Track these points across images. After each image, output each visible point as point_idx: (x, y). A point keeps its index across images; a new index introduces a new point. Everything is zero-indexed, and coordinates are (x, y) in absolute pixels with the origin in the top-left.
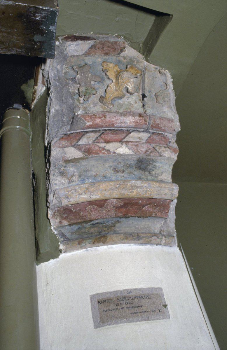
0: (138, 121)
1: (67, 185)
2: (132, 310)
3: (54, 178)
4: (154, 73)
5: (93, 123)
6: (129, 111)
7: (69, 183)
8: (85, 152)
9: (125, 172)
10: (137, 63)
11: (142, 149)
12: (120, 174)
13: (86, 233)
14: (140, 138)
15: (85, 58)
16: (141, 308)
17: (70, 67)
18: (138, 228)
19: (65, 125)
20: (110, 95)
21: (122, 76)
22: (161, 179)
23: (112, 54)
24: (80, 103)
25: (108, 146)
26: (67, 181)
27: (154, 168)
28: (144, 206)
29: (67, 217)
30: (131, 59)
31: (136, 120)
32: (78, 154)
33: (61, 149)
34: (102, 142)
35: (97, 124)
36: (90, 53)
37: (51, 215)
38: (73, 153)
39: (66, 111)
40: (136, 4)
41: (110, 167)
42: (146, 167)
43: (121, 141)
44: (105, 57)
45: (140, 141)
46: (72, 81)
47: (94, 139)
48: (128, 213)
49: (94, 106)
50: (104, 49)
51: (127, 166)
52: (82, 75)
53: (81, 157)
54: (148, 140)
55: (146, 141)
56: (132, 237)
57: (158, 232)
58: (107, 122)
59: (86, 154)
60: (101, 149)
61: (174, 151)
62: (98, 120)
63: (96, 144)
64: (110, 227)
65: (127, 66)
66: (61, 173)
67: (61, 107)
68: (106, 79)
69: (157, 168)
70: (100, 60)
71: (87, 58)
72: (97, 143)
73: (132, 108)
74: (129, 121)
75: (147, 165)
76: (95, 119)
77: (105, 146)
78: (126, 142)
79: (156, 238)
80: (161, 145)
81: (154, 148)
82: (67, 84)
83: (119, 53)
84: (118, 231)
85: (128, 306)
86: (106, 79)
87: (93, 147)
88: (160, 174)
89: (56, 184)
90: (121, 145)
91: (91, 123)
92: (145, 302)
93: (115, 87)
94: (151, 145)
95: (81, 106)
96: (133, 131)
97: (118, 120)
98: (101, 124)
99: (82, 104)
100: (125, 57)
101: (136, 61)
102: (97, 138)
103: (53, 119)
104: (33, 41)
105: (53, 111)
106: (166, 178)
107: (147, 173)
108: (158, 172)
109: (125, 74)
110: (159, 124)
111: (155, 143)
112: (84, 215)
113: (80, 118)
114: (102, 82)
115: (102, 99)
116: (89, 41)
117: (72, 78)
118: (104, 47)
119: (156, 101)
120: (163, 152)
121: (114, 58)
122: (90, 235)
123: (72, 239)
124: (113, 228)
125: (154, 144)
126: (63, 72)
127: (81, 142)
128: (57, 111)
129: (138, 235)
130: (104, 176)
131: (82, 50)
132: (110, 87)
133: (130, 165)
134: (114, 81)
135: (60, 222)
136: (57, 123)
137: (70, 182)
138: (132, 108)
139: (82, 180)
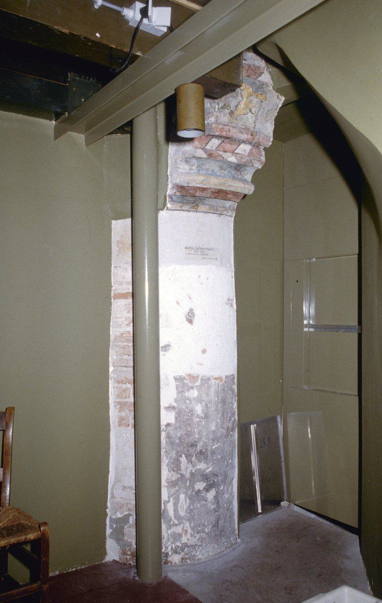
1: (188, 171)
2: (203, 257)
7: (190, 170)
14: (244, 151)
25: (224, 155)
32: (204, 155)
43: (233, 152)
72: (219, 150)
74: (244, 137)
78: (236, 153)
85: (201, 253)
92: (210, 252)
95: (215, 114)
96: (242, 142)
107: (239, 173)
108: (245, 172)
127: (208, 147)
134: (245, 100)
135: (175, 193)
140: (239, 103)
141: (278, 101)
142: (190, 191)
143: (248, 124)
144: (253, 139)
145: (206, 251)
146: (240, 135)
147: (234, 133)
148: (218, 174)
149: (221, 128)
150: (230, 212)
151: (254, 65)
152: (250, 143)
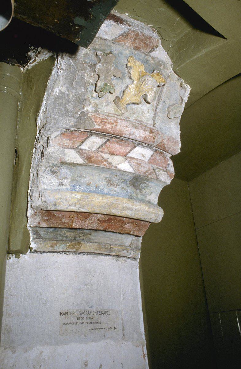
0: (147, 137)
2: (92, 326)
3: (44, 175)
4: (175, 83)
5: (102, 127)
6: (140, 120)
7: (59, 185)
8: (86, 159)
9: (118, 186)
10: (163, 68)
11: (143, 169)
12: (113, 187)
13: (61, 235)
14: (143, 156)
15: (112, 45)
16: (99, 325)
17: (93, 49)
18: (112, 239)
19: (68, 116)
20: (127, 98)
21: (147, 82)
22: (149, 199)
23: (143, 51)
24: (92, 97)
26: (57, 182)
27: (146, 187)
28: (126, 224)
29: (48, 220)
30: (159, 63)
31: (146, 135)
32: (79, 160)
33: (61, 149)
34: (106, 153)
35: (106, 129)
36: (120, 41)
37: (31, 213)
38: (72, 156)
39: (73, 98)
40: (202, 17)
41: (106, 178)
42: (139, 185)
43: (125, 156)
44: (134, 51)
45: (143, 159)
46: (90, 68)
47: (98, 147)
48: (109, 228)
49: (107, 105)
50: (136, 41)
51: (122, 180)
52: (105, 65)
53: (80, 163)
54: (150, 159)
55: (149, 160)
56: (106, 249)
57: (128, 245)
58: (117, 130)
59: (87, 161)
60: (103, 160)
61: (170, 176)
62: (108, 126)
63: (100, 153)
64: (87, 234)
65: (153, 71)
66: (52, 172)
67: (68, 90)
68: (127, 77)
69: (149, 188)
70: (127, 52)
71: (115, 45)
72: (102, 152)
73: (144, 118)
74: (139, 134)
75: (141, 184)
76: (106, 124)
77: (108, 158)
78: (130, 158)
79: (126, 252)
80: (161, 168)
81: (154, 170)
82: (84, 69)
83: (149, 52)
84: (93, 239)
85: (89, 321)
86: (127, 77)
87: (96, 155)
88: (149, 194)
89: (44, 183)
90: (124, 160)
91: (100, 127)
92: (104, 318)
93: (134, 90)
94: (152, 166)
95: (92, 101)
96: (138, 145)
97: (128, 131)
98: (110, 130)
99: (95, 98)
100: (154, 58)
101: (163, 66)
102: (102, 145)
103: (55, 100)
104: (73, 22)
105: (58, 91)
106: (153, 198)
107: (138, 191)
108: (147, 191)
109: (150, 80)
110: (165, 145)
111: (156, 164)
112: (66, 222)
113: (90, 118)
114: (122, 79)
115: (117, 100)
116: (123, 26)
117: (91, 65)
118: (137, 39)
119: (167, 115)
120: (160, 175)
121: (143, 55)
122: (65, 238)
123: (45, 238)
124: (89, 235)
125: (155, 166)
126: (83, 53)
127: (84, 147)
128: (61, 92)
129: (111, 247)
130: (97, 187)
131: (112, 34)
132: (130, 88)
133: (125, 180)
134: (135, 82)
135: (39, 223)
136: (59, 108)
137: (60, 184)
138: (144, 118)
139: (74, 186)
140: (127, 87)
141: (181, 92)
142: (64, 220)
143: (144, 120)
144: (154, 138)
145: (96, 316)
146: (134, 130)
147: (123, 128)
148: (106, 191)
149: (103, 119)
150: (132, 252)
151: (143, 34)
152: (150, 147)
